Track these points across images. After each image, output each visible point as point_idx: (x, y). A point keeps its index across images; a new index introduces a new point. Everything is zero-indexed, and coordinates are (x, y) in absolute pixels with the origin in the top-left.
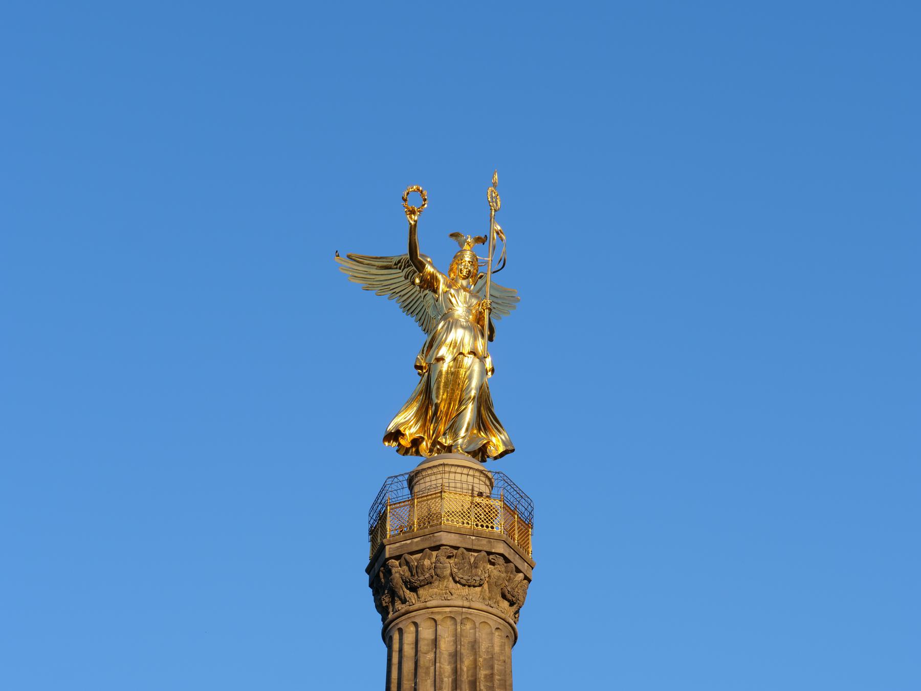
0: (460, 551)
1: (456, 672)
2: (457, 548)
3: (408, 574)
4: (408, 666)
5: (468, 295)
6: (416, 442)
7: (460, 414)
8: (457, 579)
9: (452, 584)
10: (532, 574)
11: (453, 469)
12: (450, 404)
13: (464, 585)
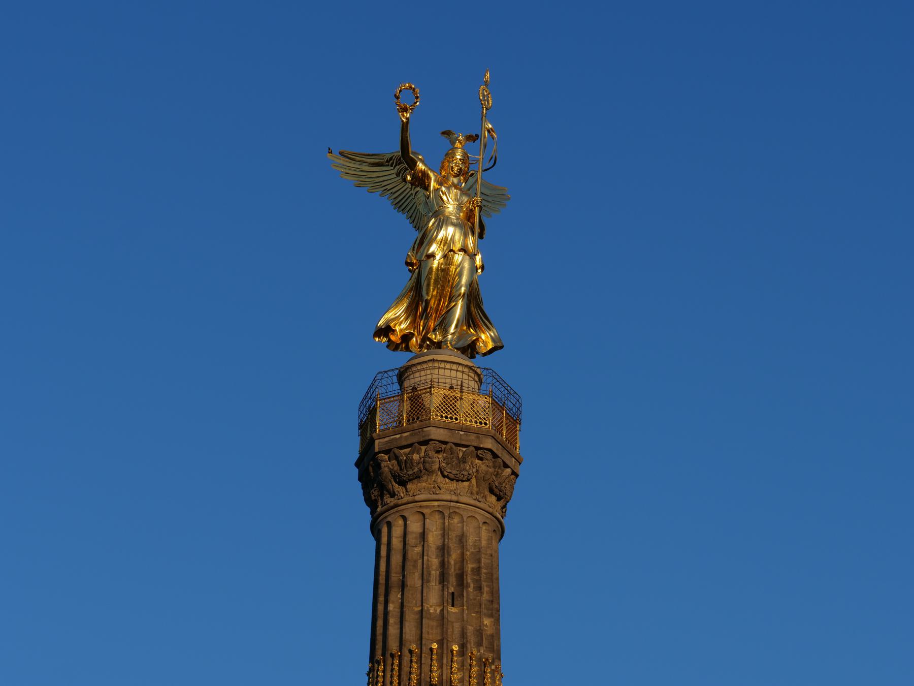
0: (448, 446)
1: (443, 565)
2: (445, 443)
3: (396, 468)
4: (396, 559)
5: (459, 192)
6: (406, 338)
7: (450, 311)
8: (446, 474)
9: (440, 479)
10: (520, 470)
11: (442, 365)
12: (440, 300)
13: (452, 480)
